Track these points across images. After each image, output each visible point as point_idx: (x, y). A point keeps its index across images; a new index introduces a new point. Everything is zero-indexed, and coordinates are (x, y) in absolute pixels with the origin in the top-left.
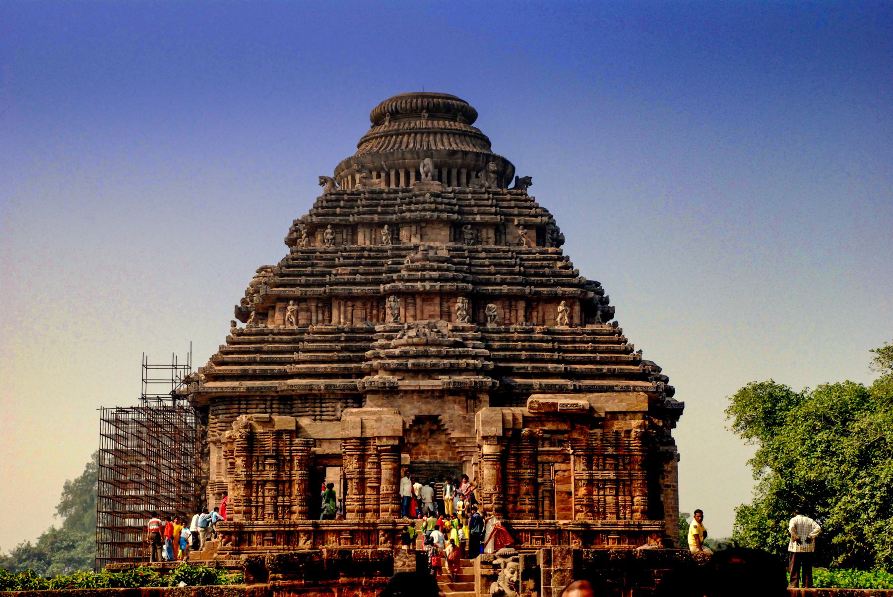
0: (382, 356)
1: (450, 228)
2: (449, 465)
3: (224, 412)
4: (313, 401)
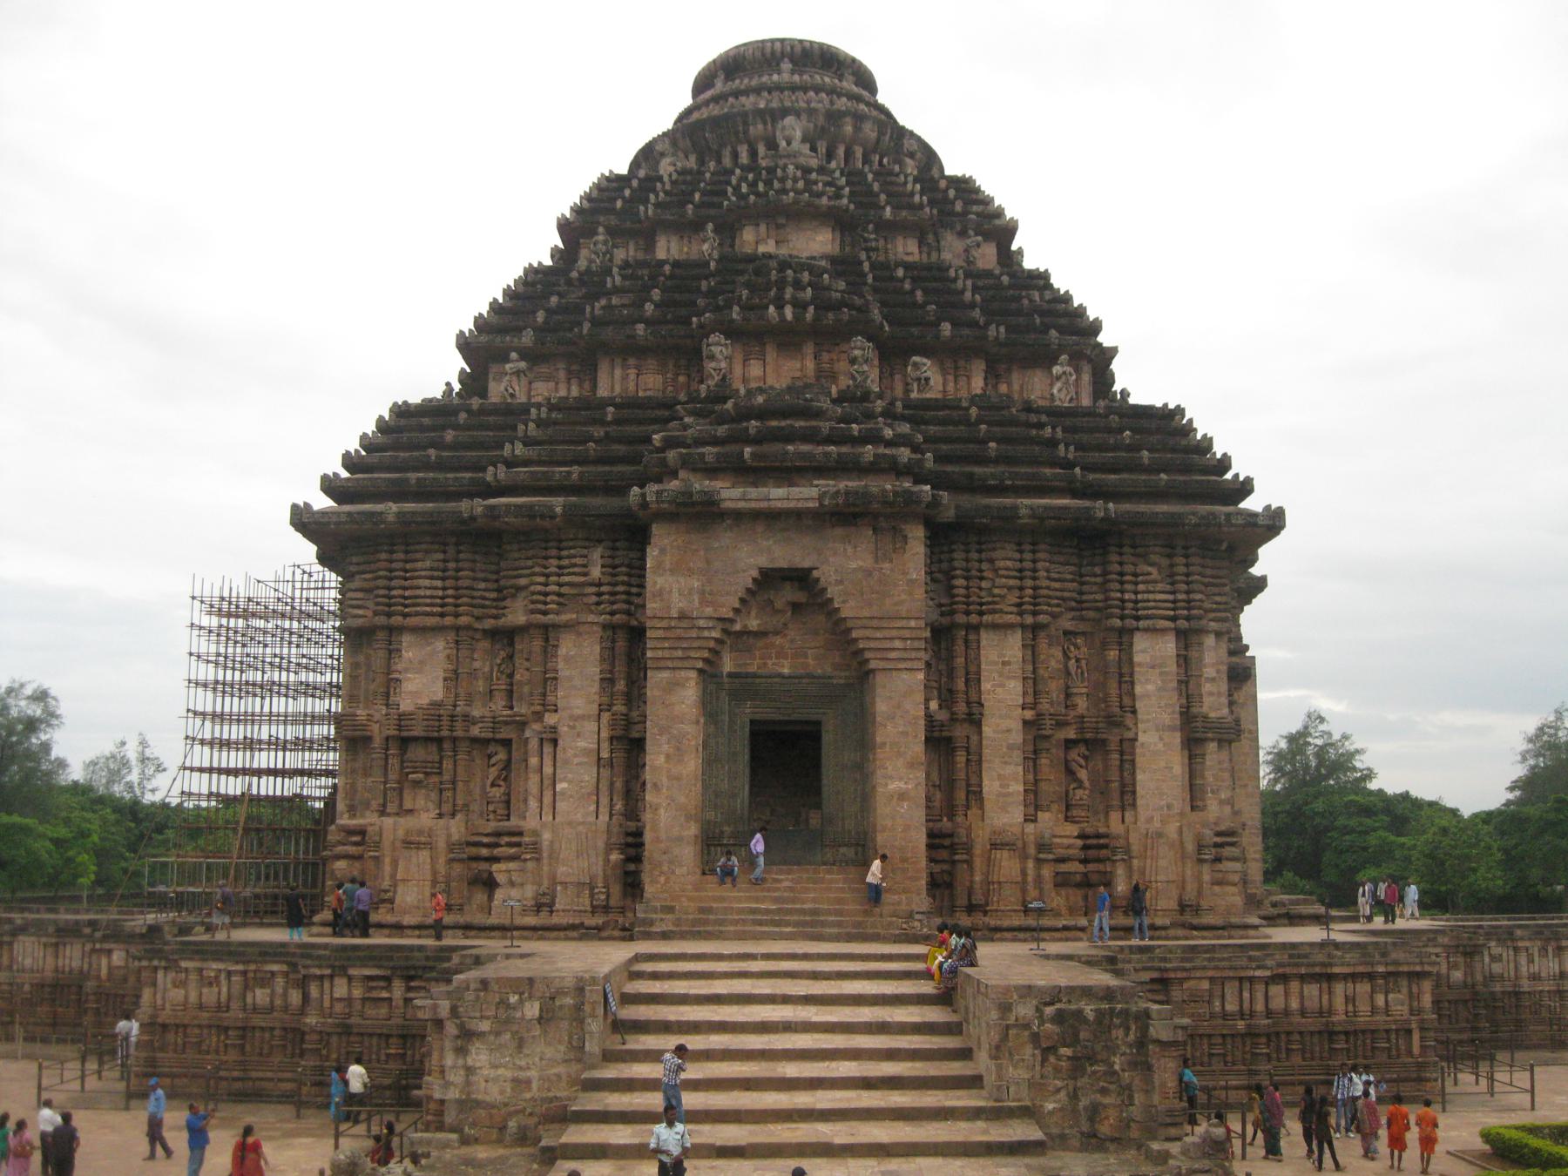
0: (689, 441)
1: (833, 230)
2: (835, 681)
3: (361, 568)
4: (544, 545)
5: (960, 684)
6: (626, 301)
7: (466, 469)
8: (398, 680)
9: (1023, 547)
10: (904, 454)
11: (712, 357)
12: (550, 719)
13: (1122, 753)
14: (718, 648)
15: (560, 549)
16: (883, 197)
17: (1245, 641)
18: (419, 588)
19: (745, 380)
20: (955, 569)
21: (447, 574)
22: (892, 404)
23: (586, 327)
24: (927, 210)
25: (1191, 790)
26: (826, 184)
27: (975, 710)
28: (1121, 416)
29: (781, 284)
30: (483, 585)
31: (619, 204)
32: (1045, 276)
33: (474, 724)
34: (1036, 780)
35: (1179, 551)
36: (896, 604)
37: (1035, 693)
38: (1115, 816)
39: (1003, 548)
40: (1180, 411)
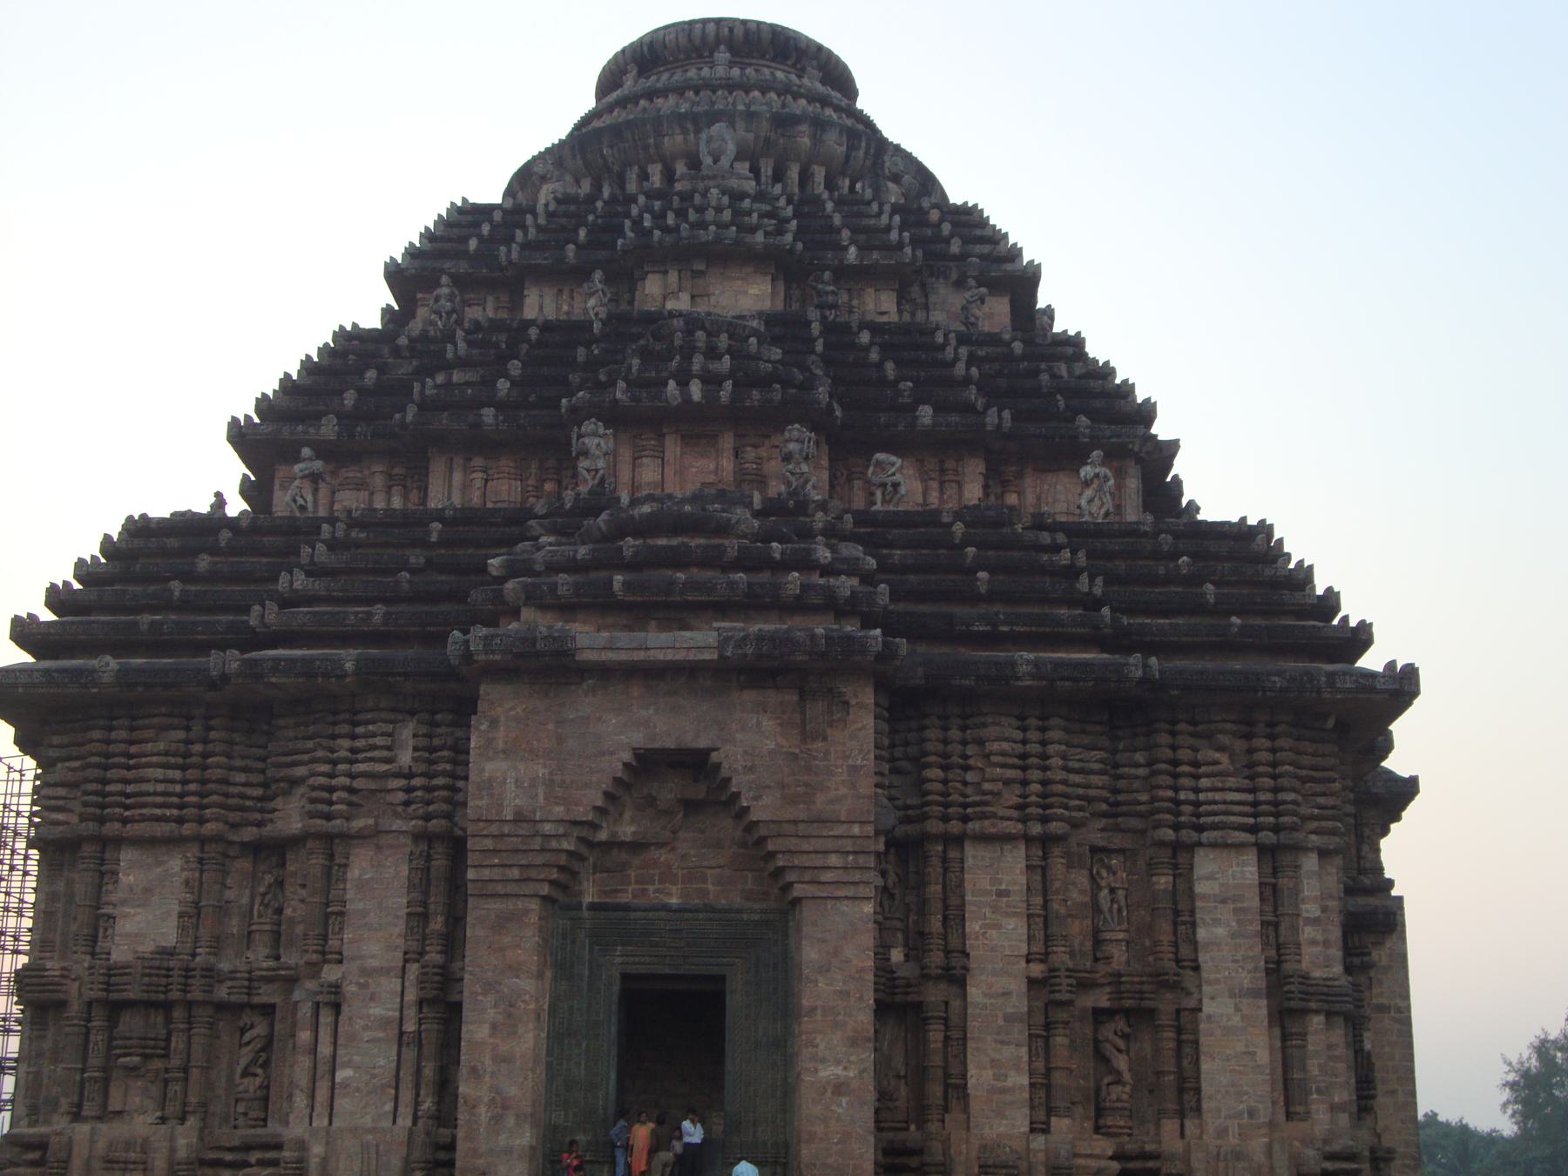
0: (538, 568)
1: (773, 280)
2: (745, 917)
4: (330, 718)
5: (935, 924)
6: (471, 376)
7: (225, 609)
8: (111, 917)
9: (1028, 722)
10: (846, 585)
11: (585, 453)
12: (331, 974)
13: (1179, 1030)
14: (576, 865)
15: (355, 724)
16: (846, 234)
17: (1387, 875)
18: (147, 781)
19: (634, 487)
20: (925, 754)
21: (188, 761)
22: (840, 518)
23: (411, 412)
24: (908, 250)
25: (1286, 1089)
26: (770, 215)
27: (956, 961)
28: (1177, 536)
29: (688, 352)
30: (241, 777)
31: (473, 244)
32: (1077, 342)
33: (221, 982)
34: (1049, 1070)
35: (1261, 728)
36: (831, 802)
37: (1047, 939)
38: (1170, 1126)
39: (998, 724)
40: (1265, 529)
